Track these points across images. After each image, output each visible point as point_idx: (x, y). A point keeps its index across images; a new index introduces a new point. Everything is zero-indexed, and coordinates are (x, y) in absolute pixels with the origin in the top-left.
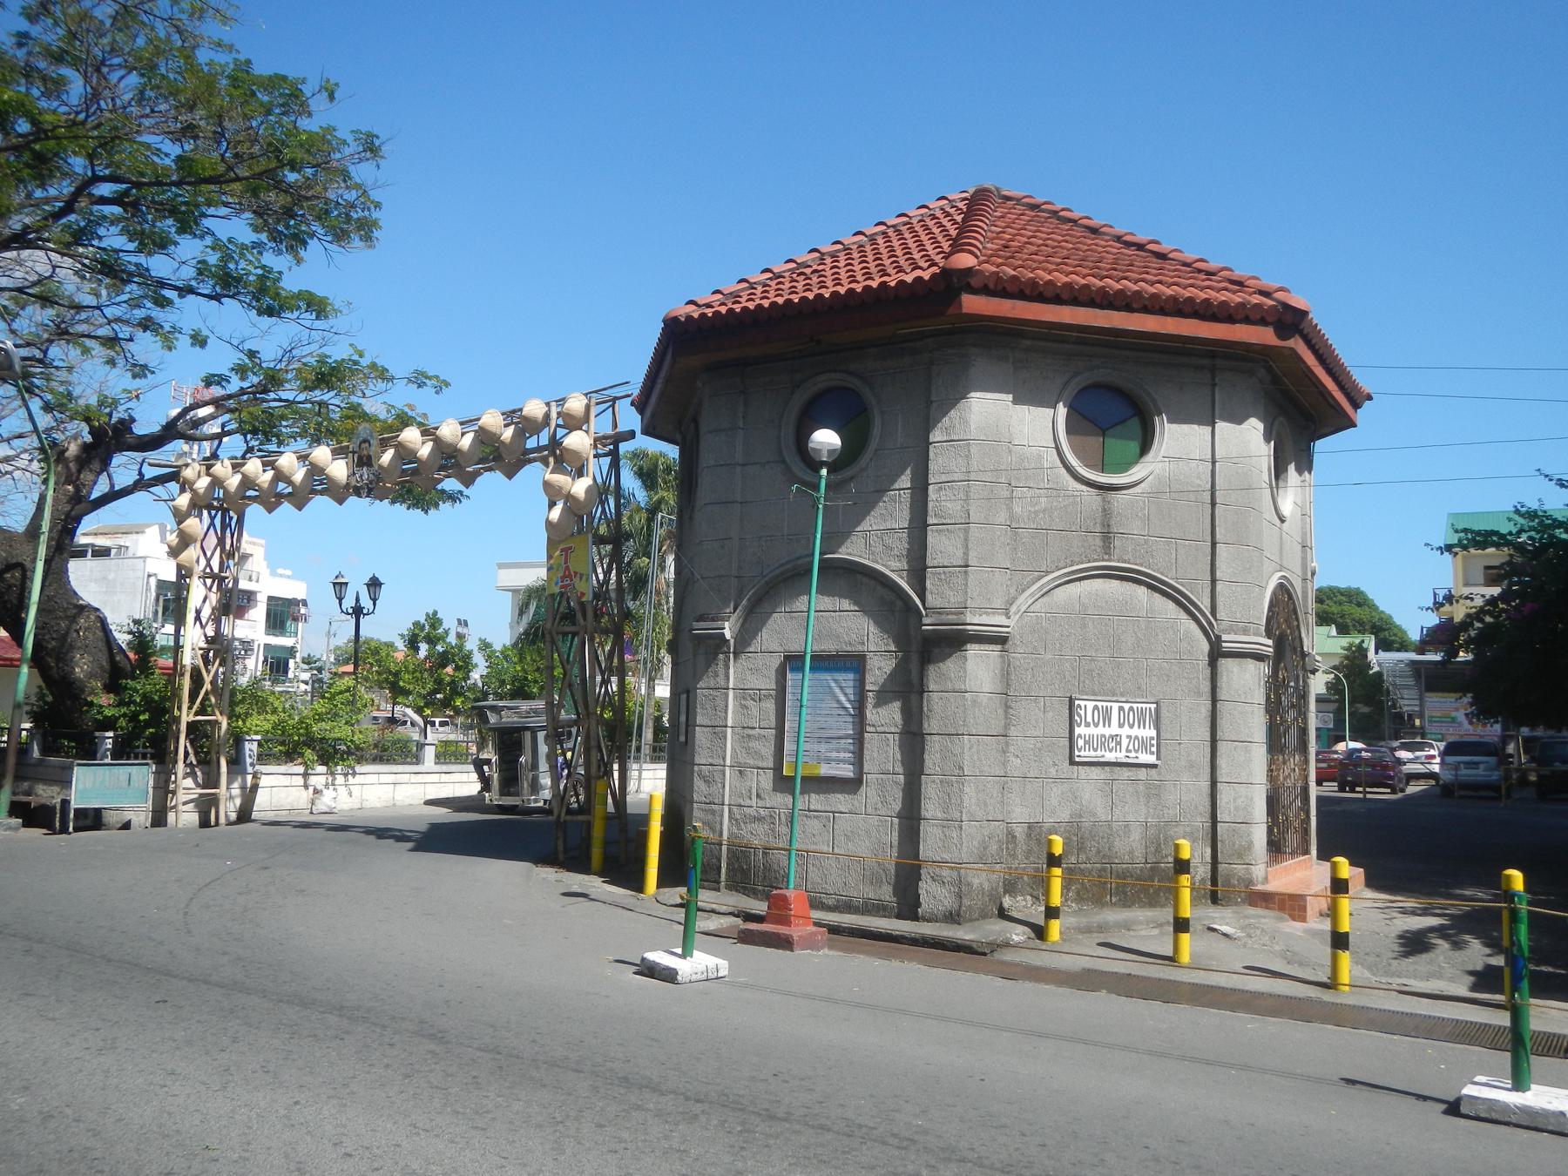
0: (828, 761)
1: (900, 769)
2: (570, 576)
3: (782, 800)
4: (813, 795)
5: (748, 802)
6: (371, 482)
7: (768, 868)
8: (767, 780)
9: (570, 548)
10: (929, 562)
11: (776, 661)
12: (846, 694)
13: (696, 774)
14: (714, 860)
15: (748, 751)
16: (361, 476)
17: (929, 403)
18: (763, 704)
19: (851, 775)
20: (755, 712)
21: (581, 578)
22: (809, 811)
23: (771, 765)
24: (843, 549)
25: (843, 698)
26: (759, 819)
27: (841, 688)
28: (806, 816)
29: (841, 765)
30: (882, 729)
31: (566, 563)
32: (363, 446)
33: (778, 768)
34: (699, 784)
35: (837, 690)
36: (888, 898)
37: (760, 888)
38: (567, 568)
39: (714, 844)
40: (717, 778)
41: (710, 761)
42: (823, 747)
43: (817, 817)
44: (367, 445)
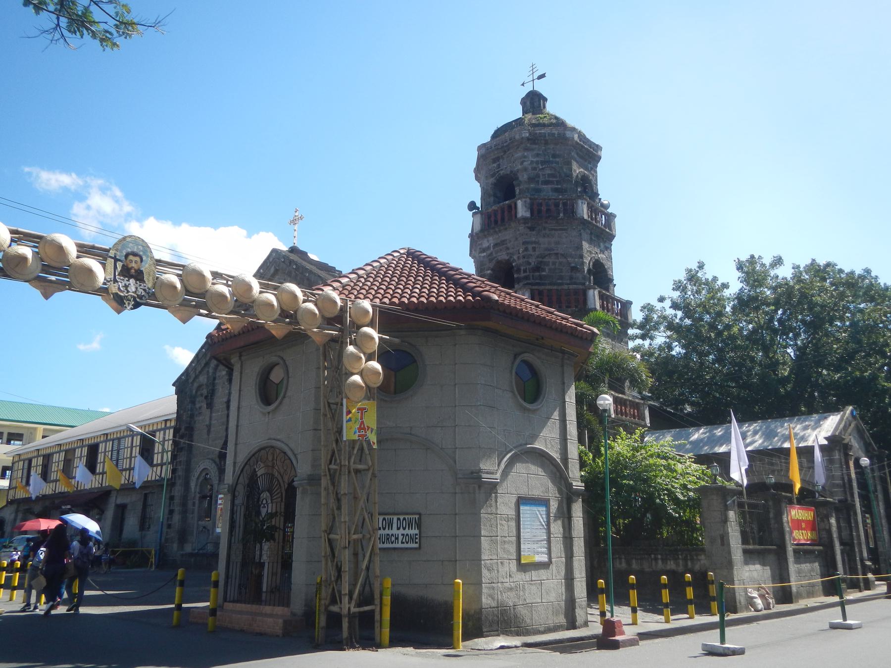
0: (538, 553)
1: (563, 555)
2: (364, 428)
3: (520, 577)
4: (533, 572)
5: (506, 580)
6: (141, 297)
7: (516, 617)
8: (513, 565)
9: (365, 409)
10: (569, 457)
11: (514, 500)
12: (542, 518)
13: (483, 566)
14: (495, 618)
15: (504, 549)
16: (126, 286)
17: (564, 383)
18: (509, 523)
19: (546, 560)
20: (506, 528)
21: (372, 432)
22: (532, 581)
23: (515, 558)
24: (536, 443)
25: (542, 520)
26: (511, 589)
27: (541, 515)
28: (531, 584)
29: (543, 555)
30: (555, 536)
31: (362, 418)
32: (131, 257)
33: (519, 559)
34: (485, 572)
35: (539, 516)
36: (563, 621)
37: (513, 629)
38: (362, 423)
39: (494, 608)
40: (494, 568)
41: (491, 557)
42: (535, 546)
43: (535, 584)
44: (138, 259)
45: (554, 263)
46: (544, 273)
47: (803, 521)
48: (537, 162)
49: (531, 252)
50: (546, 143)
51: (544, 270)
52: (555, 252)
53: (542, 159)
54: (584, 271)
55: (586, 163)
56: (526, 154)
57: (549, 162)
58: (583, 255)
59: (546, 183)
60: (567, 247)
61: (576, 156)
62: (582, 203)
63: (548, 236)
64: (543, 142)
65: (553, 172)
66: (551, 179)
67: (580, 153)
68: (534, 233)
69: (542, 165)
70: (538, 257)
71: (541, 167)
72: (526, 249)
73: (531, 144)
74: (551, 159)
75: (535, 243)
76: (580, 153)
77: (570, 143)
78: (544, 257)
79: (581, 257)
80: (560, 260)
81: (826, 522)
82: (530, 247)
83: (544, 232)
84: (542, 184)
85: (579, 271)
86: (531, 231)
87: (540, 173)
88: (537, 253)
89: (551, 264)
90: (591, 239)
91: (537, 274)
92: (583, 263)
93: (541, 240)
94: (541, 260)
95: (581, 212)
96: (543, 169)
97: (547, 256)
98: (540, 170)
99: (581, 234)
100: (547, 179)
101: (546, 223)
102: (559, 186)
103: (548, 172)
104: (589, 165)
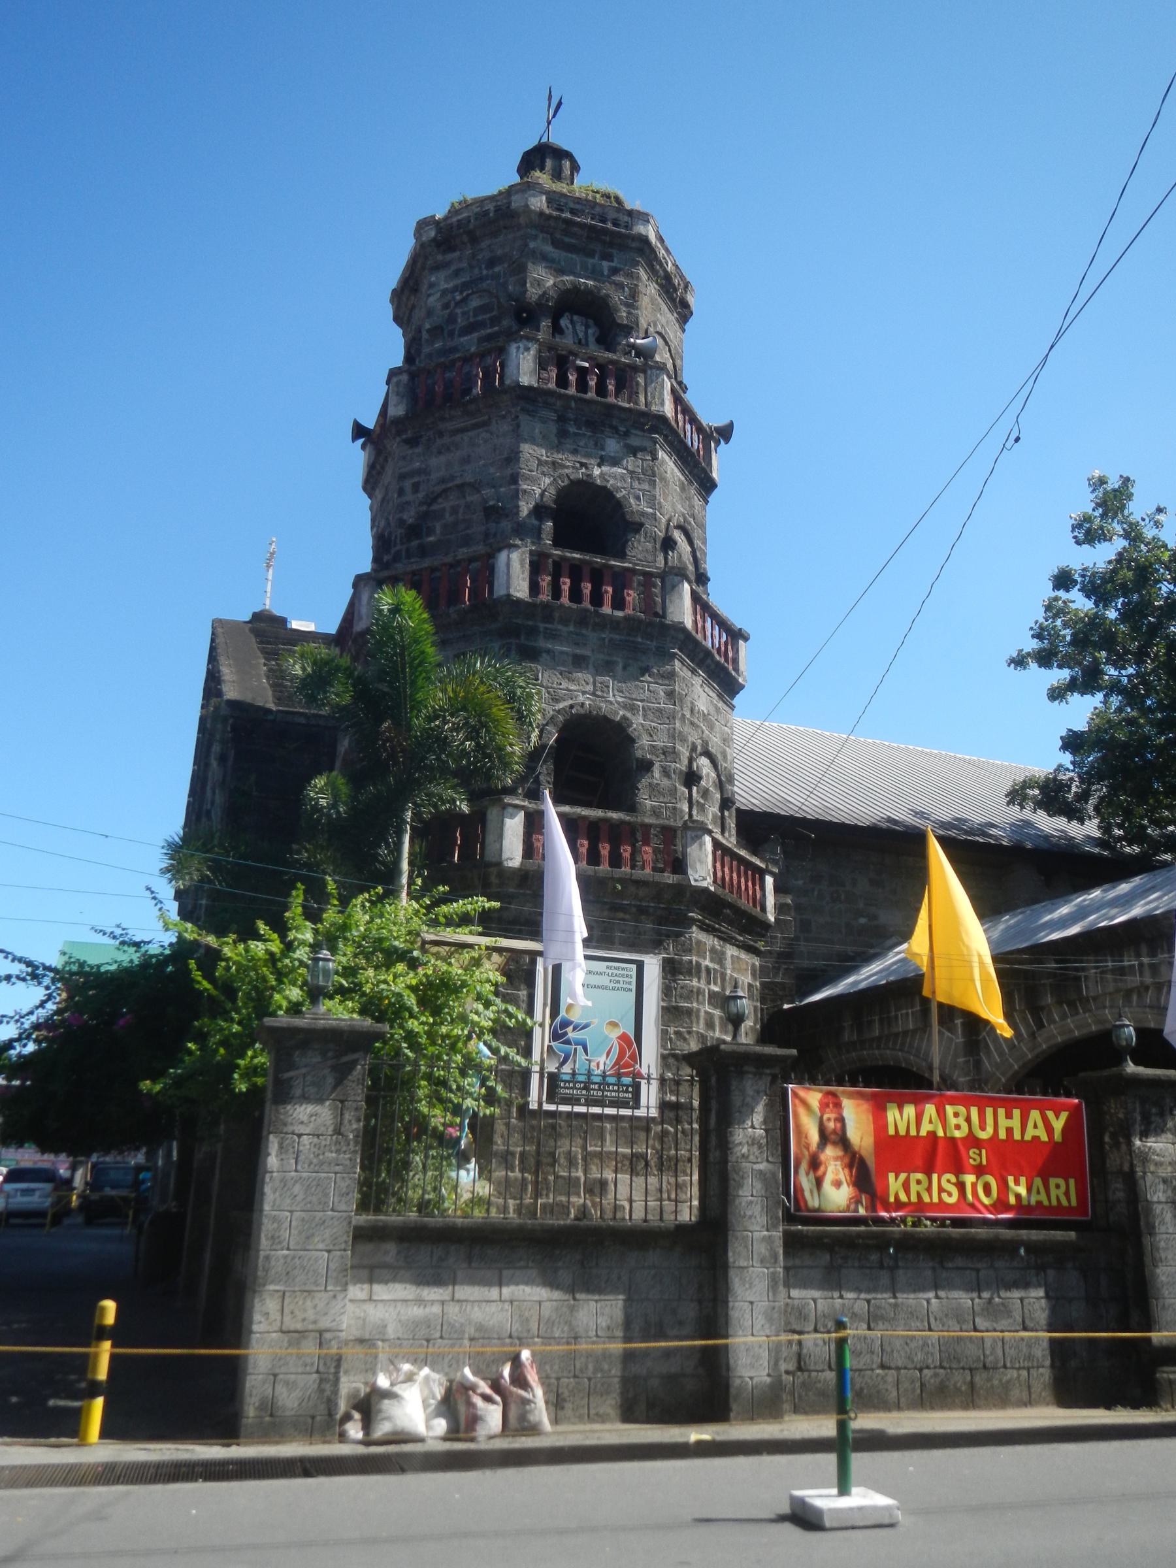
45: (454, 510)
46: (431, 539)
47: (973, 1141)
48: (455, 289)
49: (409, 497)
50: (474, 240)
51: (431, 531)
52: (458, 481)
53: (465, 278)
54: (517, 513)
55: (591, 261)
56: (433, 279)
57: (482, 279)
58: (518, 474)
59: (470, 329)
60: (484, 465)
61: (548, 249)
62: (518, 348)
63: (448, 449)
64: (465, 238)
65: (485, 300)
66: (480, 318)
67: (567, 240)
68: (419, 450)
69: (461, 293)
70: (421, 504)
71: (458, 298)
72: (401, 492)
73: (444, 252)
74: (485, 272)
75: (419, 472)
76: (567, 240)
77: (522, 220)
78: (435, 500)
79: (514, 479)
80: (469, 499)
81: (1124, 1147)
82: (408, 484)
83: (439, 442)
84: (460, 336)
85: (507, 516)
86: (411, 447)
87: (459, 311)
88: (421, 495)
89: (447, 515)
90: (562, 434)
91: (415, 543)
92: (515, 496)
93: (434, 462)
94: (424, 508)
95: (515, 372)
96: (464, 300)
97: (439, 495)
98: (457, 304)
99: (518, 426)
100: (471, 320)
101: (443, 419)
102: (496, 328)
103: (475, 303)
104: (605, 264)
